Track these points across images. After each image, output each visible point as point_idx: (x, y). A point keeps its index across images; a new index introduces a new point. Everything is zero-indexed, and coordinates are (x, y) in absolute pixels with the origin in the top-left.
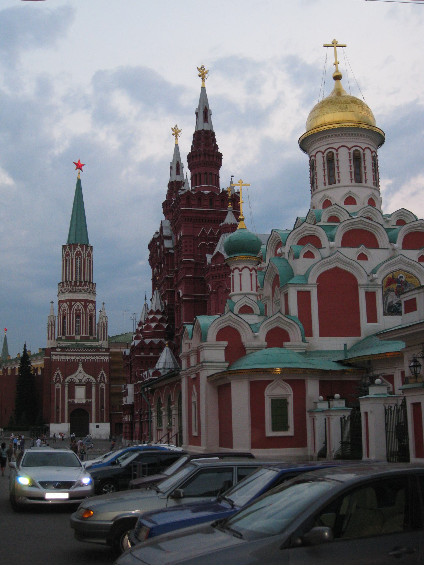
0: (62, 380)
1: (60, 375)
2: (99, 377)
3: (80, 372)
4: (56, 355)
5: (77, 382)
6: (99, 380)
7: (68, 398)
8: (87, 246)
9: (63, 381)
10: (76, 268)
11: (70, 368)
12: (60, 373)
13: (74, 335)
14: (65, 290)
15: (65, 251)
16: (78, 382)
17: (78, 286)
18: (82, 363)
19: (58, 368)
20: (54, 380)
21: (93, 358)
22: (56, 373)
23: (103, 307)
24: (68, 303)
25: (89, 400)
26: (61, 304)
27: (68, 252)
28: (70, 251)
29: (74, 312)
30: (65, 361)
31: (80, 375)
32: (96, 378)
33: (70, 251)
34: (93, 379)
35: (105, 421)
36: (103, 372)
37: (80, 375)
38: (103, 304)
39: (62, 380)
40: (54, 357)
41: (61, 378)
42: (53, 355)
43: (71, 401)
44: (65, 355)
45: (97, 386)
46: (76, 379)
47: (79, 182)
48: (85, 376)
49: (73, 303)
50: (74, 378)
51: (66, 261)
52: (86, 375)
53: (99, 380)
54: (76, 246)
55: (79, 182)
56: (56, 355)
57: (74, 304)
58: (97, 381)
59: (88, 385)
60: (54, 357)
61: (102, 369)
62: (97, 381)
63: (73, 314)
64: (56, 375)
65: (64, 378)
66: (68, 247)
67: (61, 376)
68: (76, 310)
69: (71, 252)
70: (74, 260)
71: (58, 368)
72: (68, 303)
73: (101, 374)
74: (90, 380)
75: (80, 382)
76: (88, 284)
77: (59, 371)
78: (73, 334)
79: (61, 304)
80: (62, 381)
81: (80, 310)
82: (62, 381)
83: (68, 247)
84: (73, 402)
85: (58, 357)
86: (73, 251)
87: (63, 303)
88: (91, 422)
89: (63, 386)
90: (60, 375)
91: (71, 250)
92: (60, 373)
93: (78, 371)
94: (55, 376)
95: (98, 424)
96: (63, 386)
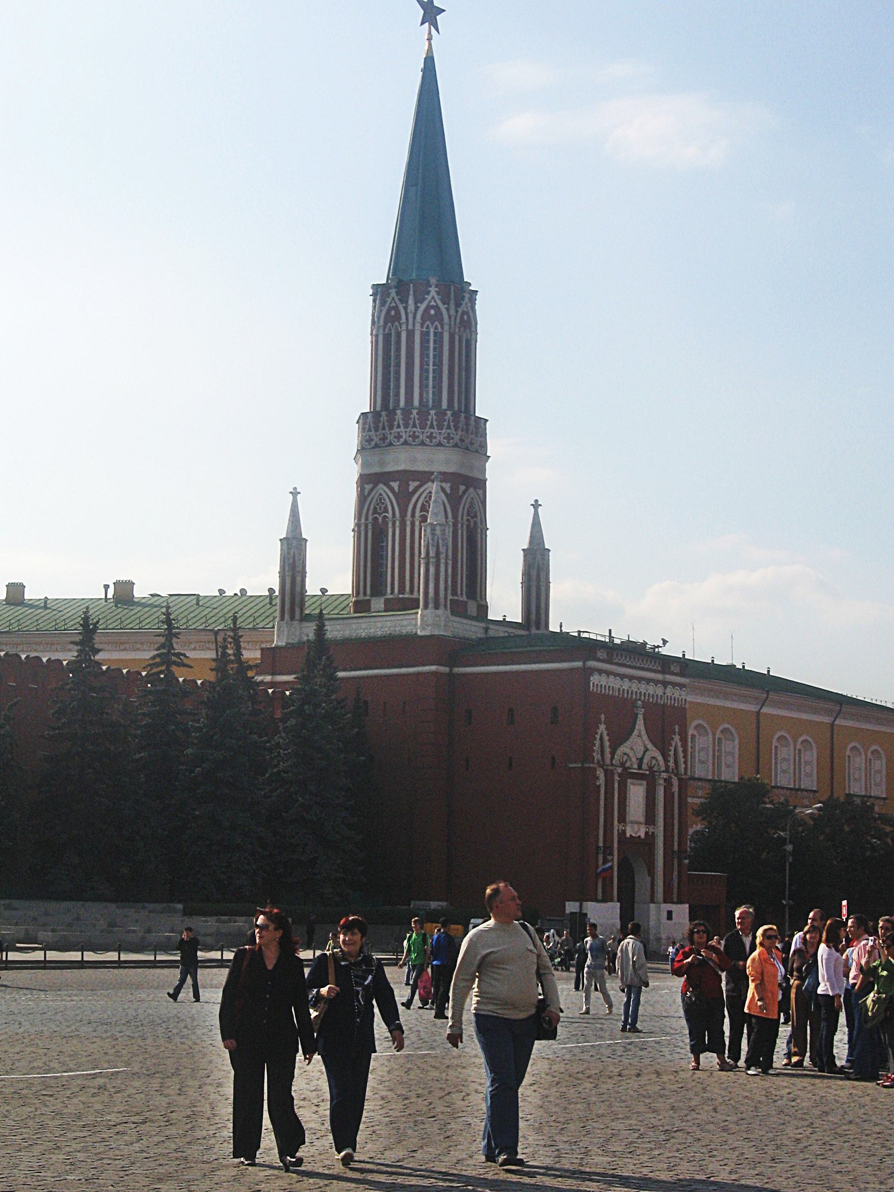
0: (608, 756)
1: (606, 738)
4: (600, 672)
8: (459, 296)
10: (460, 369)
12: (605, 733)
13: (464, 598)
14: (431, 437)
15: (418, 301)
16: (635, 766)
17: (414, 426)
18: (645, 705)
21: (659, 690)
24: (447, 486)
26: (413, 485)
27: (436, 308)
28: (443, 308)
29: (465, 518)
31: (638, 745)
33: (443, 308)
34: (660, 758)
35: (675, 900)
36: (677, 738)
37: (638, 745)
38: (536, 505)
39: (608, 756)
41: (608, 750)
44: (616, 675)
46: (631, 754)
48: (646, 750)
49: (462, 488)
50: (628, 751)
51: (425, 336)
52: (650, 746)
56: (600, 672)
57: (464, 492)
59: (650, 779)
60: (595, 679)
62: (667, 767)
63: (462, 527)
65: (613, 754)
66: (433, 290)
67: (607, 744)
68: (468, 515)
69: (448, 309)
70: (457, 338)
71: (603, 716)
72: (447, 486)
74: (654, 762)
75: (640, 767)
77: (602, 727)
78: (462, 594)
79: (413, 485)
80: (608, 761)
81: (476, 516)
82: (608, 761)
86: (452, 306)
88: (652, 901)
90: (606, 738)
93: (636, 732)
95: (670, 907)
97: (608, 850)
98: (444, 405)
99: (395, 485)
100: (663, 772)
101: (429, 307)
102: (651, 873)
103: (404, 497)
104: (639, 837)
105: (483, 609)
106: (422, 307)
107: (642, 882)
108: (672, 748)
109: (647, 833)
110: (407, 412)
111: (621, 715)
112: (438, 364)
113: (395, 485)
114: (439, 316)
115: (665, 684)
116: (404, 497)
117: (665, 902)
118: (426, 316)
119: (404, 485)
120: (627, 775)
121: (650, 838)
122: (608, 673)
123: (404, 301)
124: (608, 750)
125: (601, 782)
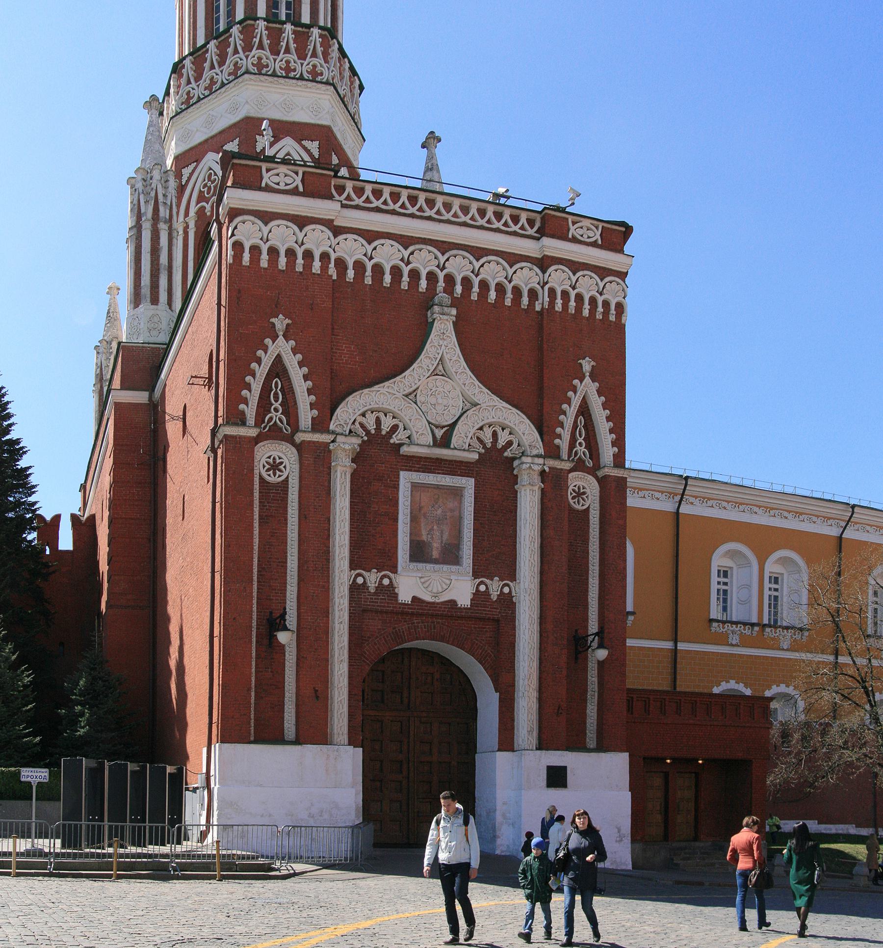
0: (306, 415)
1: (297, 374)
2: (568, 421)
3: (440, 371)
5: (421, 443)
6: (563, 444)
7: (353, 566)
9: (320, 425)
12: (292, 362)
19: (280, 323)
20: (250, 411)
22: (267, 360)
25: (495, 587)
30: (332, 271)
31: (438, 395)
32: (545, 427)
34: (525, 431)
36: (588, 388)
37: (438, 395)
39: (306, 415)
40: (249, 232)
41: (304, 401)
42: (234, 213)
43: (372, 585)
45: (553, 484)
53: (563, 444)
58: (552, 452)
61: (587, 365)
62: (552, 452)
64: (262, 371)
65: (328, 403)
71: (280, 323)
73: (576, 401)
84: (390, 592)
85: (282, 236)
89: (316, 461)
90: (297, 374)
92: (292, 362)
94: (257, 386)
96: (316, 461)
100: (538, 456)
104: (453, 603)
108: (571, 411)
109: (477, 594)
120: (380, 457)
122: (302, 222)
124: (304, 401)
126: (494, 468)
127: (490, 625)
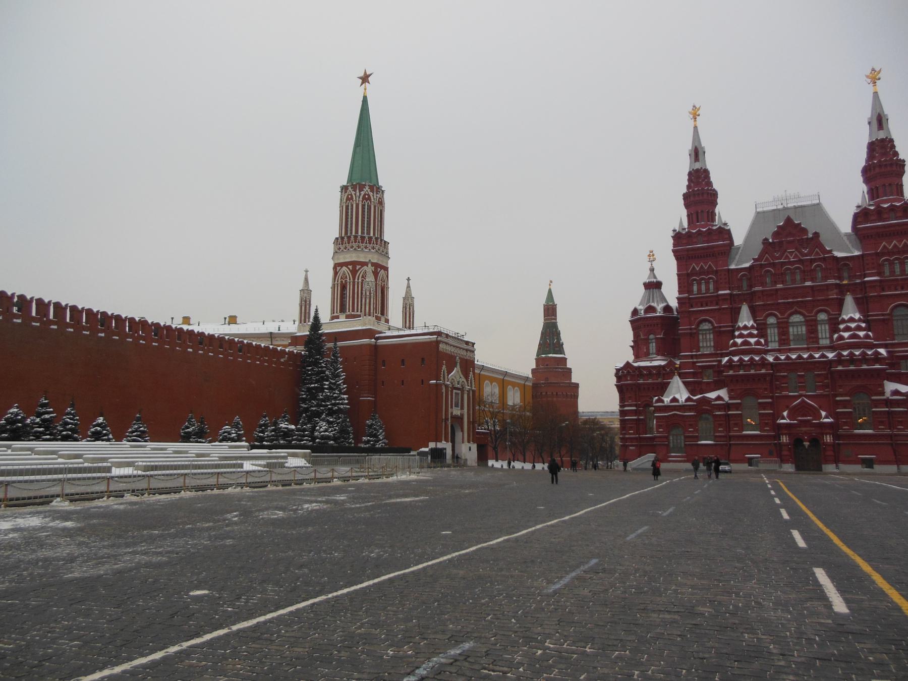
11: (451, 362)
15: (360, 191)
23: (408, 284)
26: (358, 267)
27: (368, 195)
28: (371, 194)
32: (467, 381)
33: (371, 194)
38: (408, 279)
47: (365, 100)
51: (363, 206)
54: (362, 187)
55: (365, 100)
66: (367, 188)
76: (381, 245)
83: (367, 188)
87: (362, 266)
91: (372, 191)
95: (469, 445)
97: (447, 419)
98: (372, 235)
99: (350, 267)
101: (365, 195)
102: (462, 431)
103: (354, 272)
105: (387, 321)
106: (363, 193)
107: (459, 435)
110: (356, 237)
111: (451, 362)
112: (369, 218)
113: (350, 267)
114: (369, 198)
115: (467, 350)
116: (354, 272)
117: (469, 442)
118: (364, 198)
119: (354, 267)
121: (462, 415)
123: (355, 191)
125: (444, 390)
126: (462, 390)
127: (460, 419)
